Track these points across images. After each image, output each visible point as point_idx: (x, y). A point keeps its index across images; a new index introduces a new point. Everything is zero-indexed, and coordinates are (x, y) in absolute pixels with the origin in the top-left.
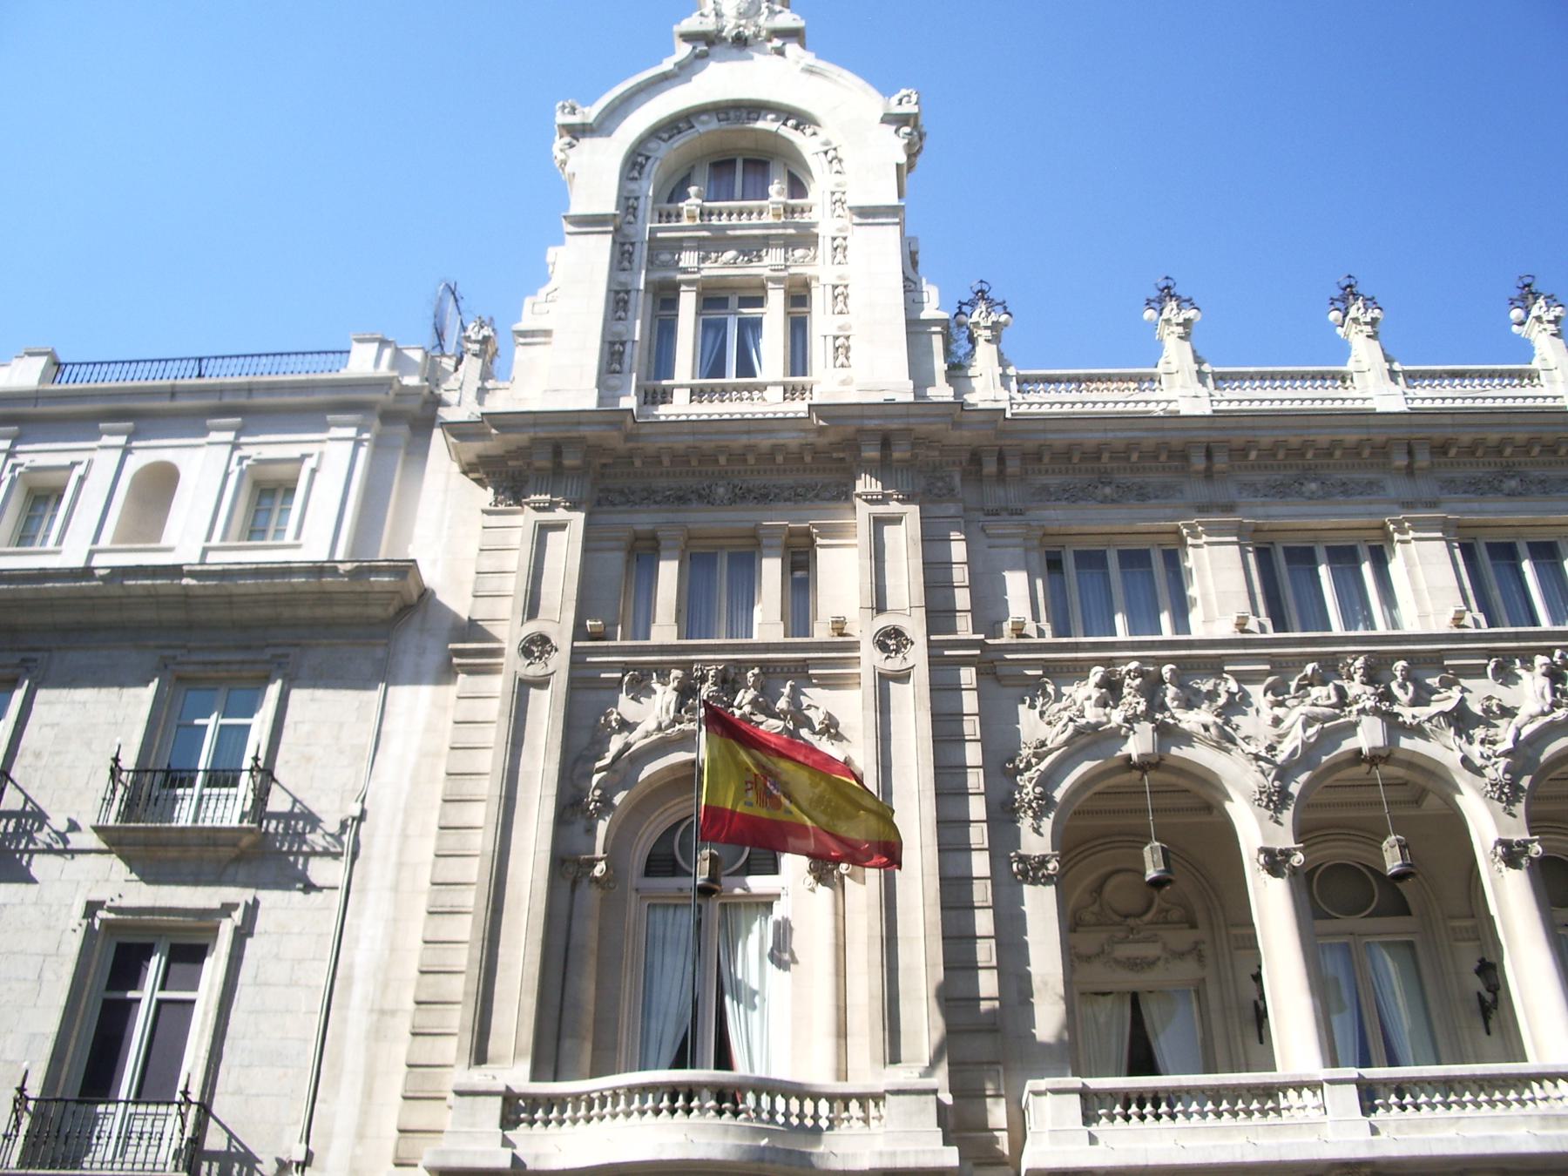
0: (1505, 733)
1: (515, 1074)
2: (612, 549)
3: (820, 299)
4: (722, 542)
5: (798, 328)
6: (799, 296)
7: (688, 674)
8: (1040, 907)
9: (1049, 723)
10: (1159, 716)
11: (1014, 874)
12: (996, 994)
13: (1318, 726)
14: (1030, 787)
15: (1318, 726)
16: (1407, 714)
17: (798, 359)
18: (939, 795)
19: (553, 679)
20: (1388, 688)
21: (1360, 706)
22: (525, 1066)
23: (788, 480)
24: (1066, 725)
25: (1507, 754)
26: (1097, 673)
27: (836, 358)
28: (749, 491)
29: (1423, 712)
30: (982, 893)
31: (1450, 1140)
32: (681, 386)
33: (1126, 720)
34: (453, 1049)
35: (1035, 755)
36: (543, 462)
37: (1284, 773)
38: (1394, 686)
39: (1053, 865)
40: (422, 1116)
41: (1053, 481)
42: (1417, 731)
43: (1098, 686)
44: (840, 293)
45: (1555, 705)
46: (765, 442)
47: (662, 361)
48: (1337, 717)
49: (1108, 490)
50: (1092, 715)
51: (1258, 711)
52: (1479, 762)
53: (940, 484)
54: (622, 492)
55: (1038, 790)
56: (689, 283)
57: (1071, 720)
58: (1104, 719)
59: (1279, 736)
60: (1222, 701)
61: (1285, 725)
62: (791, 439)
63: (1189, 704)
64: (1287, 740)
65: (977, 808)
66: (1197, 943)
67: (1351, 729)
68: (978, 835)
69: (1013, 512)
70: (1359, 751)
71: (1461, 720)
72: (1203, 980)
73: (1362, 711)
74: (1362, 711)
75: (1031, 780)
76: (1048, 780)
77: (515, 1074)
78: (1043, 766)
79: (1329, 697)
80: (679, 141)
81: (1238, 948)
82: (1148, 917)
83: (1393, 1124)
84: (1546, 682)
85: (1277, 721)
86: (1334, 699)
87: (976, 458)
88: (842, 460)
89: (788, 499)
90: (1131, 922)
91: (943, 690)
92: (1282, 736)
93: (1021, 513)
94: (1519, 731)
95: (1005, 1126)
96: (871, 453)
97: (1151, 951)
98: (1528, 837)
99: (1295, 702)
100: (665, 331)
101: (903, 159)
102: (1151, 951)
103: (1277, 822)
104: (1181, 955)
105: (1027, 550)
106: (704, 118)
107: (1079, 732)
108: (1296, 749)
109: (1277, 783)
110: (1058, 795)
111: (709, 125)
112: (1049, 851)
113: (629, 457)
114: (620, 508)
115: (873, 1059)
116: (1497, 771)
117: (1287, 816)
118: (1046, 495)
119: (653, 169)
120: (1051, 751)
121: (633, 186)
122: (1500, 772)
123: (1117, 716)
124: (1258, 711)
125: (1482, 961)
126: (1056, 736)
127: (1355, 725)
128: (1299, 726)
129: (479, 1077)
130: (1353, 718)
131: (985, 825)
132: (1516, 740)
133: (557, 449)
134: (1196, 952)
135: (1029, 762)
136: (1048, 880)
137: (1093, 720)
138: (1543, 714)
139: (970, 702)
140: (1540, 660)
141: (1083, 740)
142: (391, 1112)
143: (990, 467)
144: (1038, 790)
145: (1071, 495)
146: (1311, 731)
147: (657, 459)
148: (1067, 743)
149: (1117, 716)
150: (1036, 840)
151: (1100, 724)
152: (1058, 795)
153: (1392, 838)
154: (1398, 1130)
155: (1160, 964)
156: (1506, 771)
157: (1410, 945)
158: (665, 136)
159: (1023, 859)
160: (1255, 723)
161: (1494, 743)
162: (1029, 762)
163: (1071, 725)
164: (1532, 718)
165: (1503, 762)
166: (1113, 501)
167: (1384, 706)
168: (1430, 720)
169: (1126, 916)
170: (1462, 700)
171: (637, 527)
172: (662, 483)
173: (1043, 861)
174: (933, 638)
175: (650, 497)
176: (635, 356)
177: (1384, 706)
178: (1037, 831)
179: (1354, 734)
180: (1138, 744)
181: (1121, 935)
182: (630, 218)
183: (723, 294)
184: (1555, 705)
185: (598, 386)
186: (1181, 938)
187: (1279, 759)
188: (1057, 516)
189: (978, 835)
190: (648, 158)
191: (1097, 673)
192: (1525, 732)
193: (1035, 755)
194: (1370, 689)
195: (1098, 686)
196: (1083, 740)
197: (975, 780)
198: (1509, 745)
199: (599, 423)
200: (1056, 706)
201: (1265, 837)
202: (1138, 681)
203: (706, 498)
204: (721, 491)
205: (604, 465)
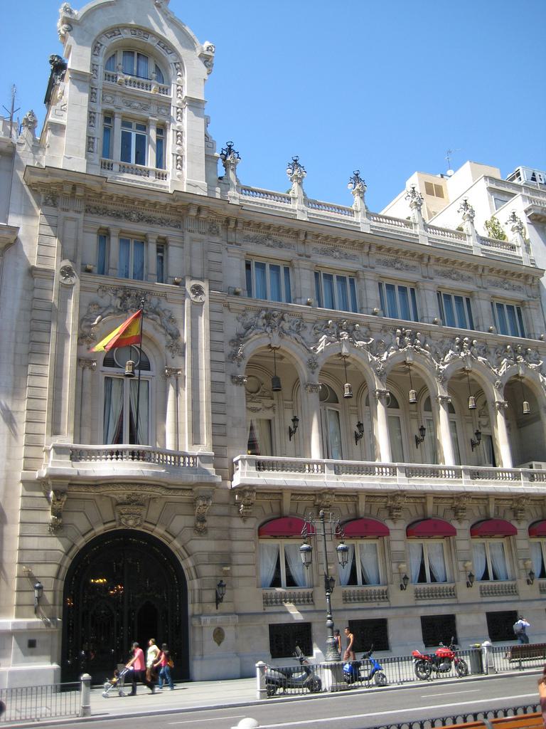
1: (67, 440)
2: (93, 233)
3: (170, 135)
4: (131, 236)
5: (160, 144)
6: (161, 130)
7: (125, 293)
17: (160, 162)
19: (74, 288)
22: (71, 438)
23: (159, 215)
27: (177, 165)
28: (144, 217)
32: (116, 163)
34: (44, 428)
36: (68, 190)
40: (33, 452)
41: (252, 234)
44: (179, 135)
46: (153, 200)
47: (107, 151)
49: (270, 242)
53: (214, 229)
54: (95, 208)
56: (119, 114)
62: (164, 200)
66: (274, 405)
69: (237, 244)
72: (274, 418)
77: (67, 440)
80: (114, 40)
82: (257, 394)
87: (228, 221)
88: (180, 212)
89: (159, 224)
93: (240, 245)
96: (193, 213)
97: (258, 406)
100: (108, 131)
101: (206, 77)
102: (258, 406)
104: (269, 408)
105: (241, 260)
106: (125, 31)
111: (126, 35)
113: (101, 195)
114: (94, 215)
115: (189, 443)
118: (248, 239)
119: (103, 50)
121: (95, 59)
125: (359, 422)
129: (58, 441)
133: (74, 187)
134: (272, 407)
142: (22, 452)
143: (232, 225)
145: (257, 241)
147: (111, 197)
158: (109, 36)
166: (272, 246)
169: (252, 393)
171: (103, 225)
172: (110, 207)
175: (105, 212)
176: (98, 144)
182: (95, 76)
183: (130, 121)
185: (86, 158)
186: (268, 403)
188: (252, 248)
190: (101, 45)
199: (93, 180)
203: (128, 217)
204: (134, 216)
205: (89, 196)
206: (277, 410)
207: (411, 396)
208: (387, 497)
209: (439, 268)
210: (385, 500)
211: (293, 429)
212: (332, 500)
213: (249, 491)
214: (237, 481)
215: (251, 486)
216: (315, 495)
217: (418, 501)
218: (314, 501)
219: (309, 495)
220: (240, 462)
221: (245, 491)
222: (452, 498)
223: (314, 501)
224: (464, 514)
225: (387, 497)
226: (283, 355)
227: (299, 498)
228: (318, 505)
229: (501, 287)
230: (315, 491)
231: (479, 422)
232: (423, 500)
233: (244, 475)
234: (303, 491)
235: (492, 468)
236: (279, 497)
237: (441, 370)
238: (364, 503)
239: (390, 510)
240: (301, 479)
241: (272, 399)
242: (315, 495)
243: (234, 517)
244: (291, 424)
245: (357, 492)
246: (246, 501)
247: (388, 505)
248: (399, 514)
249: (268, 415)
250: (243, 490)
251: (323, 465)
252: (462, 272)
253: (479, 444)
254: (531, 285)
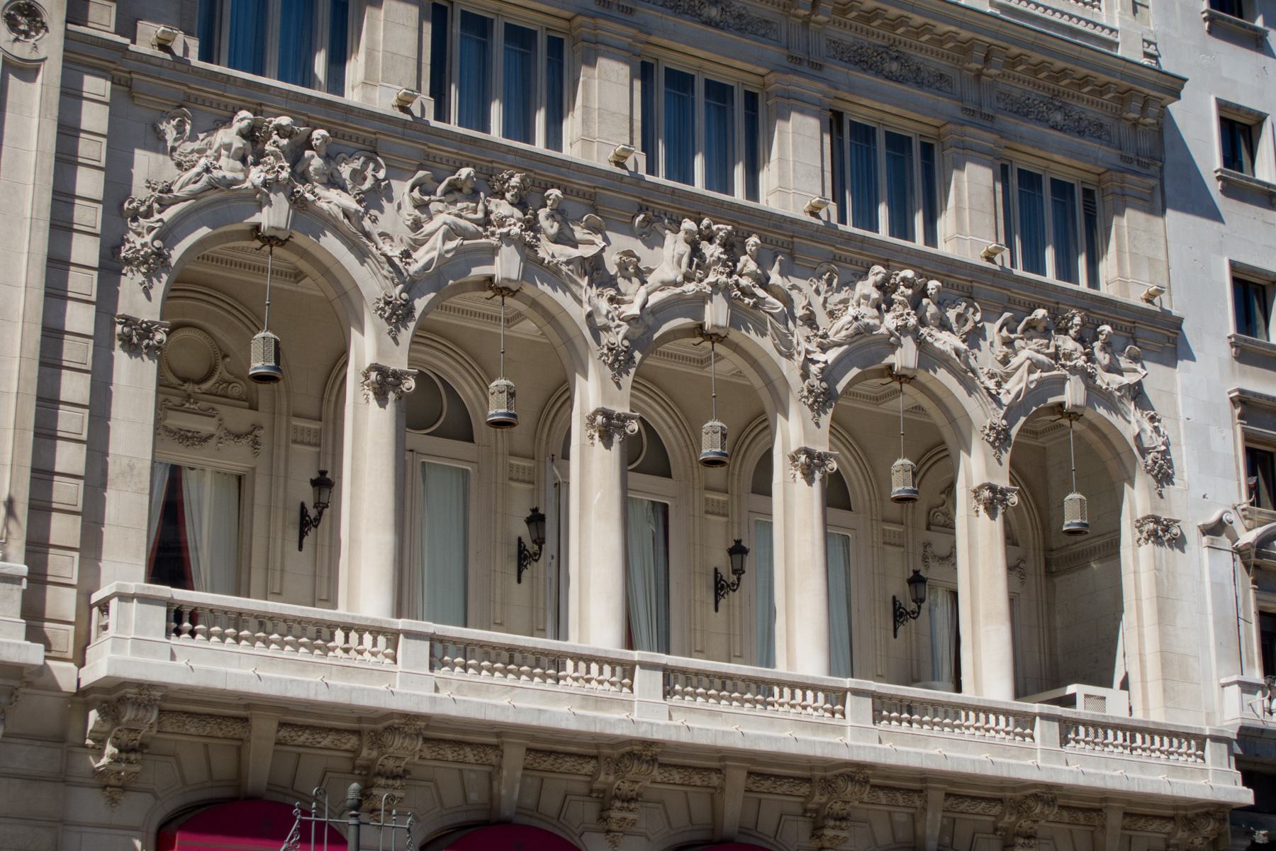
0: (636, 298)
8: (134, 380)
9: (179, 165)
10: (300, 188)
11: (119, 335)
12: (82, 473)
13: (457, 242)
14: (148, 238)
15: (457, 242)
16: (548, 250)
18: (53, 226)
20: (536, 216)
21: (505, 230)
24: (199, 174)
25: (631, 320)
26: (244, 117)
29: (563, 252)
30: (76, 352)
31: (504, 708)
33: (265, 183)
35: (159, 200)
37: (413, 286)
38: (542, 213)
39: (160, 336)
42: (552, 274)
43: (242, 134)
45: (688, 278)
48: (478, 235)
50: (228, 168)
51: (399, 207)
52: (600, 321)
55: (158, 243)
57: (207, 170)
58: (241, 176)
59: (415, 241)
60: (367, 185)
61: (428, 228)
63: (333, 182)
64: (422, 250)
65: (85, 250)
66: (256, 427)
67: (490, 254)
68: (82, 283)
70: (490, 279)
71: (593, 269)
72: (253, 469)
73: (506, 238)
74: (506, 238)
75: (150, 229)
76: (169, 234)
78: (168, 214)
79: (475, 212)
81: (295, 442)
82: (206, 386)
83: (455, 684)
84: (686, 249)
85: (416, 225)
86: (480, 215)
90: (189, 387)
91: (71, 95)
92: (417, 244)
94: (649, 294)
95: (73, 619)
97: (204, 426)
98: (627, 411)
99: (440, 206)
102: (204, 426)
103: (395, 339)
104: (238, 436)
107: (213, 186)
108: (433, 259)
109: (404, 296)
110: (176, 254)
112: (157, 319)
116: (617, 337)
117: (406, 335)
120: (177, 200)
122: (620, 336)
123: (256, 175)
124: (399, 207)
125: (535, 510)
126: (184, 183)
127: (494, 251)
128: (441, 233)
130: (494, 241)
131: (95, 274)
132: (643, 307)
134: (250, 435)
135: (150, 207)
136: (153, 351)
137: (229, 175)
138: (675, 284)
139: (94, 117)
140: (688, 224)
141: (214, 195)
144: (158, 243)
146: (451, 245)
148: (194, 195)
149: (256, 175)
150: (140, 299)
151: (235, 181)
152: (176, 254)
153: (501, 382)
154: (459, 690)
155: (213, 441)
156: (625, 338)
157: (465, 473)
159: (128, 321)
160: (394, 218)
161: (620, 302)
162: (150, 207)
163: (206, 177)
164: (665, 284)
165: (625, 328)
167: (528, 236)
168: (568, 263)
169: (185, 380)
170: (603, 249)
173: (147, 331)
174: (71, 27)
177: (528, 236)
178: (147, 292)
179: (491, 262)
180: (274, 216)
181: (176, 400)
184: (688, 278)
186: (239, 418)
187: (413, 268)
189: (82, 283)
191: (244, 117)
192: (653, 299)
193: (159, 200)
194: (518, 213)
195: (242, 134)
196: (214, 195)
197: (87, 215)
198: (634, 310)
200: (189, 146)
201: (380, 351)
202: (285, 142)
206: (264, 448)
207: (705, 439)
208: (595, 757)
209: (847, 37)
210: (589, 767)
211: (312, 513)
212: (403, 749)
213: (138, 704)
214: (103, 663)
215: (141, 686)
216: (357, 732)
217: (697, 779)
218: (356, 752)
219: (338, 731)
220: (114, 603)
221: (122, 700)
222: (808, 780)
223: (356, 752)
224: (843, 834)
225: (595, 757)
226: (303, 265)
227: (304, 737)
228: (367, 768)
229: (1041, 120)
230: (360, 720)
231: (927, 545)
232: (715, 779)
233: (131, 646)
234: (321, 716)
235: (953, 697)
236: (238, 730)
237: (815, 362)
238: (519, 774)
239: (605, 800)
240: (315, 678)
241: (253, 407)
242: (357, 732)
243: (81, 785)
244: (306, 494)
245: (499, 735)
246: (125, 737)
247: (596, 786)
248: (630, 816)
249: (236, 458)
250: (115, 697)
251: (393, 637)
252: (918, 56)
253: (915, 614)
254: (1135, 124)
